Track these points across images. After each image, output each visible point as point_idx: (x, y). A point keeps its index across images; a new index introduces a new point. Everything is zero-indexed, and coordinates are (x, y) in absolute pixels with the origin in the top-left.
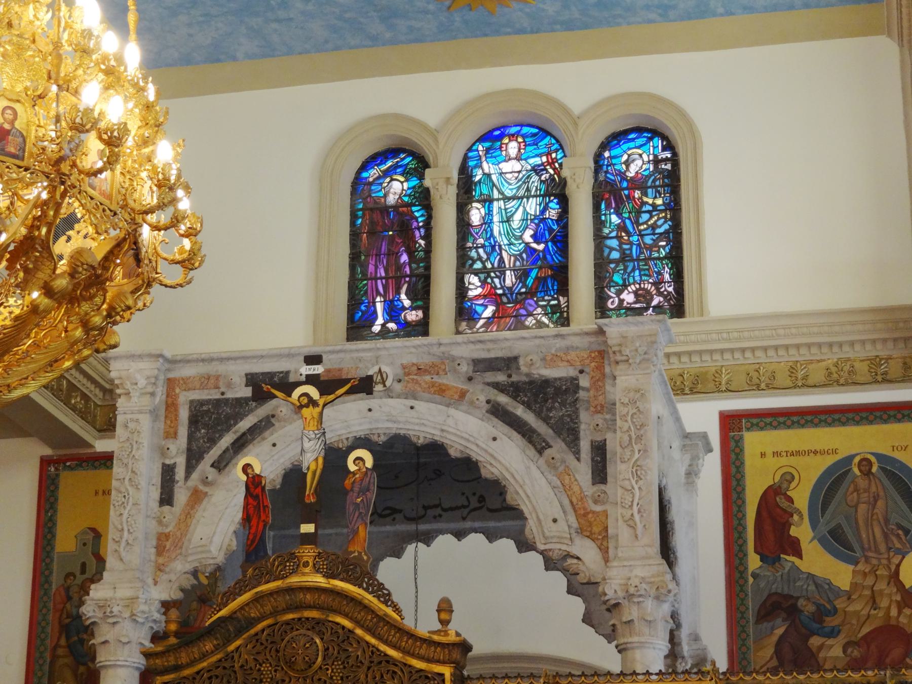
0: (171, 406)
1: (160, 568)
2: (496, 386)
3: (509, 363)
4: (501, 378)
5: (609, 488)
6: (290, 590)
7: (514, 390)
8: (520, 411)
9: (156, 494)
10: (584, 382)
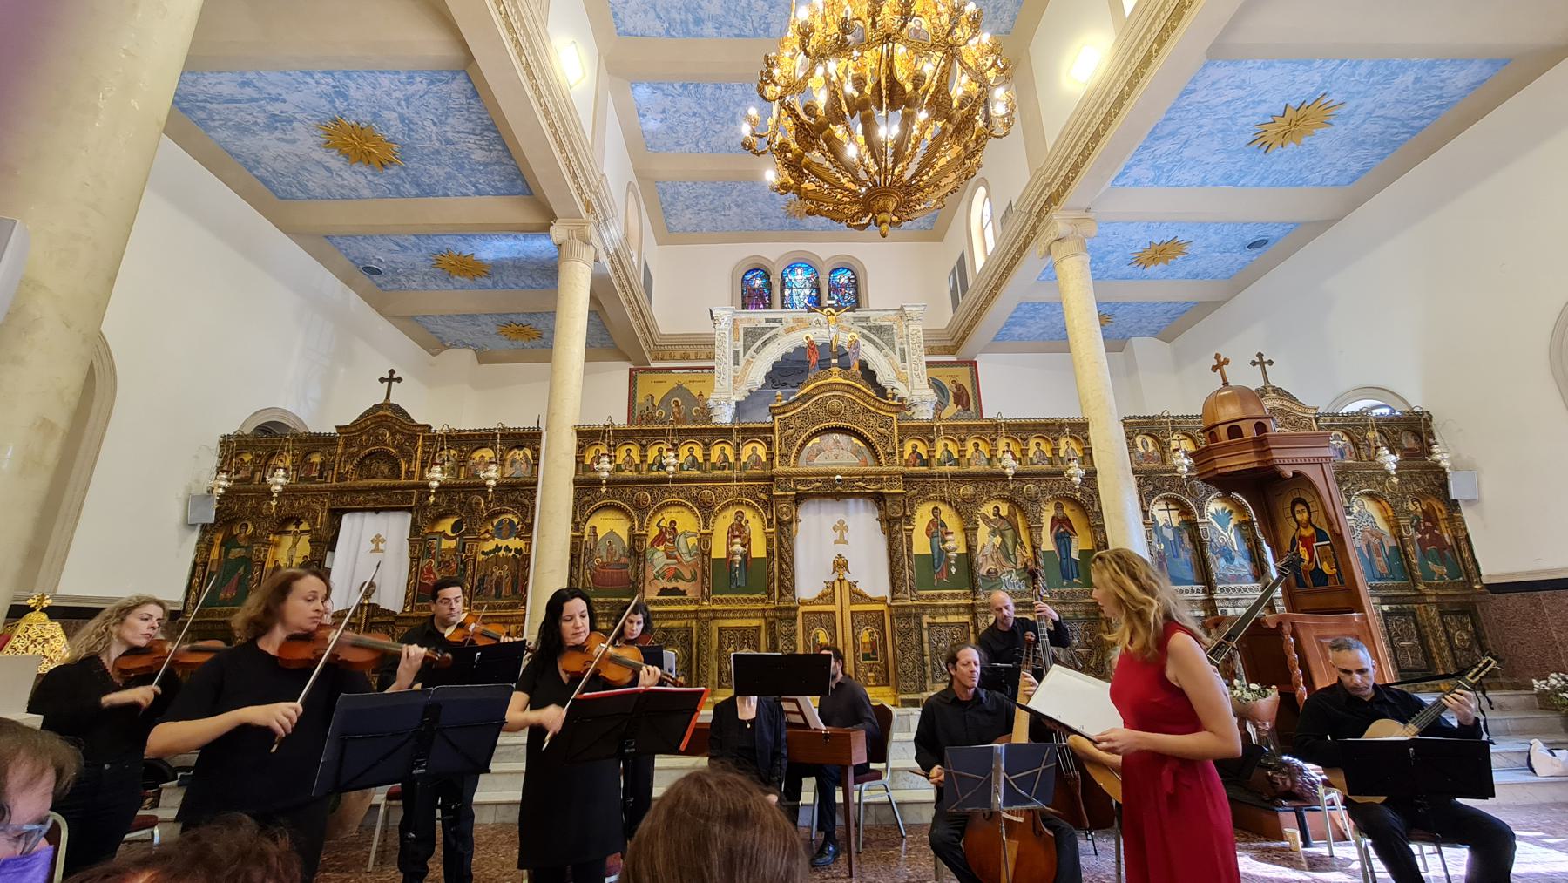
0: (736, 329)
1: (735, 389)
2: (862, 327)
3: (867, 319)
4: (864, 324)
5: (907, 364)
6: (830, 384)
7: (870, 329)
8: (872, 336)
9: (732, 361)
10: (895, 327)
